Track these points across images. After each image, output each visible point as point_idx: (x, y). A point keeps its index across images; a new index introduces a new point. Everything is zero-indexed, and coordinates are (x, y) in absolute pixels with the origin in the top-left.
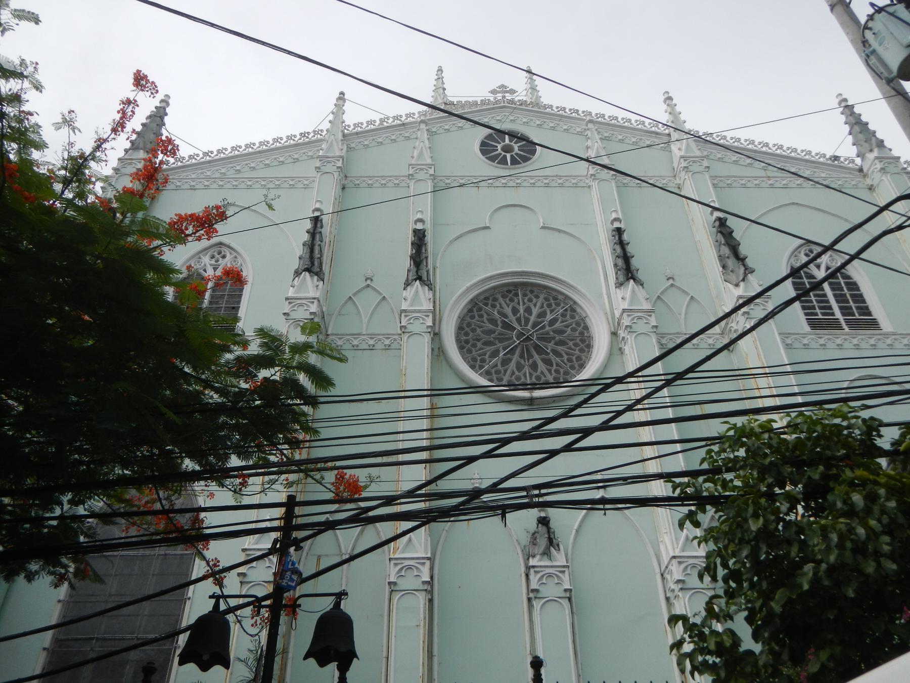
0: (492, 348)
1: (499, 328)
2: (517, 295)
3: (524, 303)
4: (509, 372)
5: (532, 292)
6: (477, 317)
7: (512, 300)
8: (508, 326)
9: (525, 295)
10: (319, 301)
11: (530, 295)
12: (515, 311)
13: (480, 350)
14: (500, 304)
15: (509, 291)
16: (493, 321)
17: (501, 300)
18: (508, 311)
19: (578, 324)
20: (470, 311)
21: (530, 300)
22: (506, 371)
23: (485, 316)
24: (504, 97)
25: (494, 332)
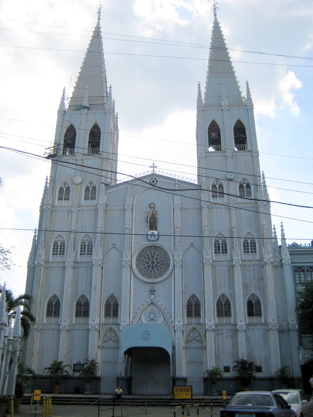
0: (144, 266)
1: (146, 260)
2: (152, 249)
3: (154, 251)
4: (148, 273)
5: (156, 248)
6: (141, 256)
7: (150, 251)
8: (149, 259)
9: (154, 249)
10: (101, 259)
11: (156, 249)
12: (151, 254)
13: (142, 266)
14: (147, 252)
15: (150, 248)
16: (145, 258)
17: (148, 250)
18: (149, 254)
19: (167, 258)
20: (139, 254)
21: (155, 250)
22: (147, 273)
24: (154, 169)
25: (145, 261)
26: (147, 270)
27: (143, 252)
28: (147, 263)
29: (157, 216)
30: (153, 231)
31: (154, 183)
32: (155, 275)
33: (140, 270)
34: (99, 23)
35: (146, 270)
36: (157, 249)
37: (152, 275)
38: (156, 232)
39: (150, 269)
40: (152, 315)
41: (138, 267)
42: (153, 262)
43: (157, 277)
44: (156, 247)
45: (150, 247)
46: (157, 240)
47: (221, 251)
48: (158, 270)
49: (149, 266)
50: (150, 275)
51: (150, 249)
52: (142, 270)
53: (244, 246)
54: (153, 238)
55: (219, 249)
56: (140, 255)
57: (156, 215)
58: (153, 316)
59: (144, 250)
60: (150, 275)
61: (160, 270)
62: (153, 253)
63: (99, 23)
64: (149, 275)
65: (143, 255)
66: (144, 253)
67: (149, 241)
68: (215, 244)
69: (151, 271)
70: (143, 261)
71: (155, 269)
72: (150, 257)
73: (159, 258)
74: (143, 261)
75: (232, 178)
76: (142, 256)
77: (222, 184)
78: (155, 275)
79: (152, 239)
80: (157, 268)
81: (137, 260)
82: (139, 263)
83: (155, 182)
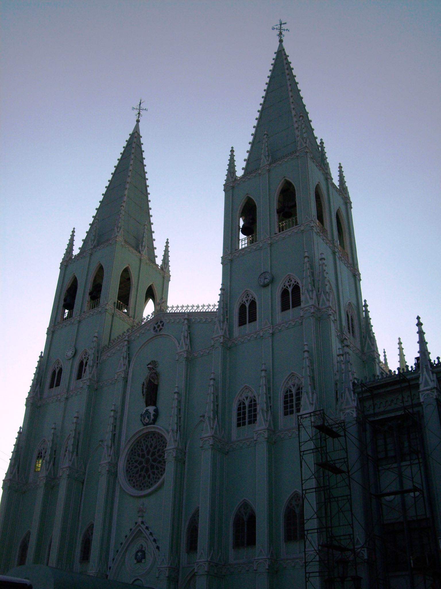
9: (151, 437)
12: (147, 447)
16: (139, 455)
18: (144, 448)
21: (153, 440)
23: (137, 452)
26: (140, 476)
27: (137, 446)
28: (141, 463)
29: (156, 381)
30: (148, 408)
31: (159, 328)
32: (149, 482)
33: (130, 476)
34: (137, 127)
35: (138, 475)
36: (155, 437)
37: (145, 483)
38: (151, 409)
39: (143, 473)
40: (139, 554)
41: (128, 472)
42: (148, 460)
43: (152, 485)
44: (154, 433)
45: (147, 436)
46: (154, 421)
47: (247, 420)
48: (154, 473)
49: (142, 470)
50: (143, 484)
51: (146, 439)
52: (133, 476)
53: (286, 402)
54: (147, 420)
55: (244, 418)
56: (132, 452)
57: (154, 380)
58: (141, 555)
59: (138, 442)
60: (143, 484)
61: (156, 471)
62: (149, 445)
63: (137, 127)
64: (141, 484)
65: (136, 451)
66: (139, 447)
67: (144, 425)
68: (239, 409)
69: (144, 477)
70: (136, 461)
71: (150, 472)
72: (145, 452)
73: (156, 453)
74: (136, 461)
75: (266, 283)
76: (135, 453)
77: (254, 299)
78: (149, 482)
79: (145, 421)
80: (153, 470)
81: (128, 461)
82: (130, 465)
83: (160, 324)
